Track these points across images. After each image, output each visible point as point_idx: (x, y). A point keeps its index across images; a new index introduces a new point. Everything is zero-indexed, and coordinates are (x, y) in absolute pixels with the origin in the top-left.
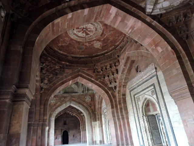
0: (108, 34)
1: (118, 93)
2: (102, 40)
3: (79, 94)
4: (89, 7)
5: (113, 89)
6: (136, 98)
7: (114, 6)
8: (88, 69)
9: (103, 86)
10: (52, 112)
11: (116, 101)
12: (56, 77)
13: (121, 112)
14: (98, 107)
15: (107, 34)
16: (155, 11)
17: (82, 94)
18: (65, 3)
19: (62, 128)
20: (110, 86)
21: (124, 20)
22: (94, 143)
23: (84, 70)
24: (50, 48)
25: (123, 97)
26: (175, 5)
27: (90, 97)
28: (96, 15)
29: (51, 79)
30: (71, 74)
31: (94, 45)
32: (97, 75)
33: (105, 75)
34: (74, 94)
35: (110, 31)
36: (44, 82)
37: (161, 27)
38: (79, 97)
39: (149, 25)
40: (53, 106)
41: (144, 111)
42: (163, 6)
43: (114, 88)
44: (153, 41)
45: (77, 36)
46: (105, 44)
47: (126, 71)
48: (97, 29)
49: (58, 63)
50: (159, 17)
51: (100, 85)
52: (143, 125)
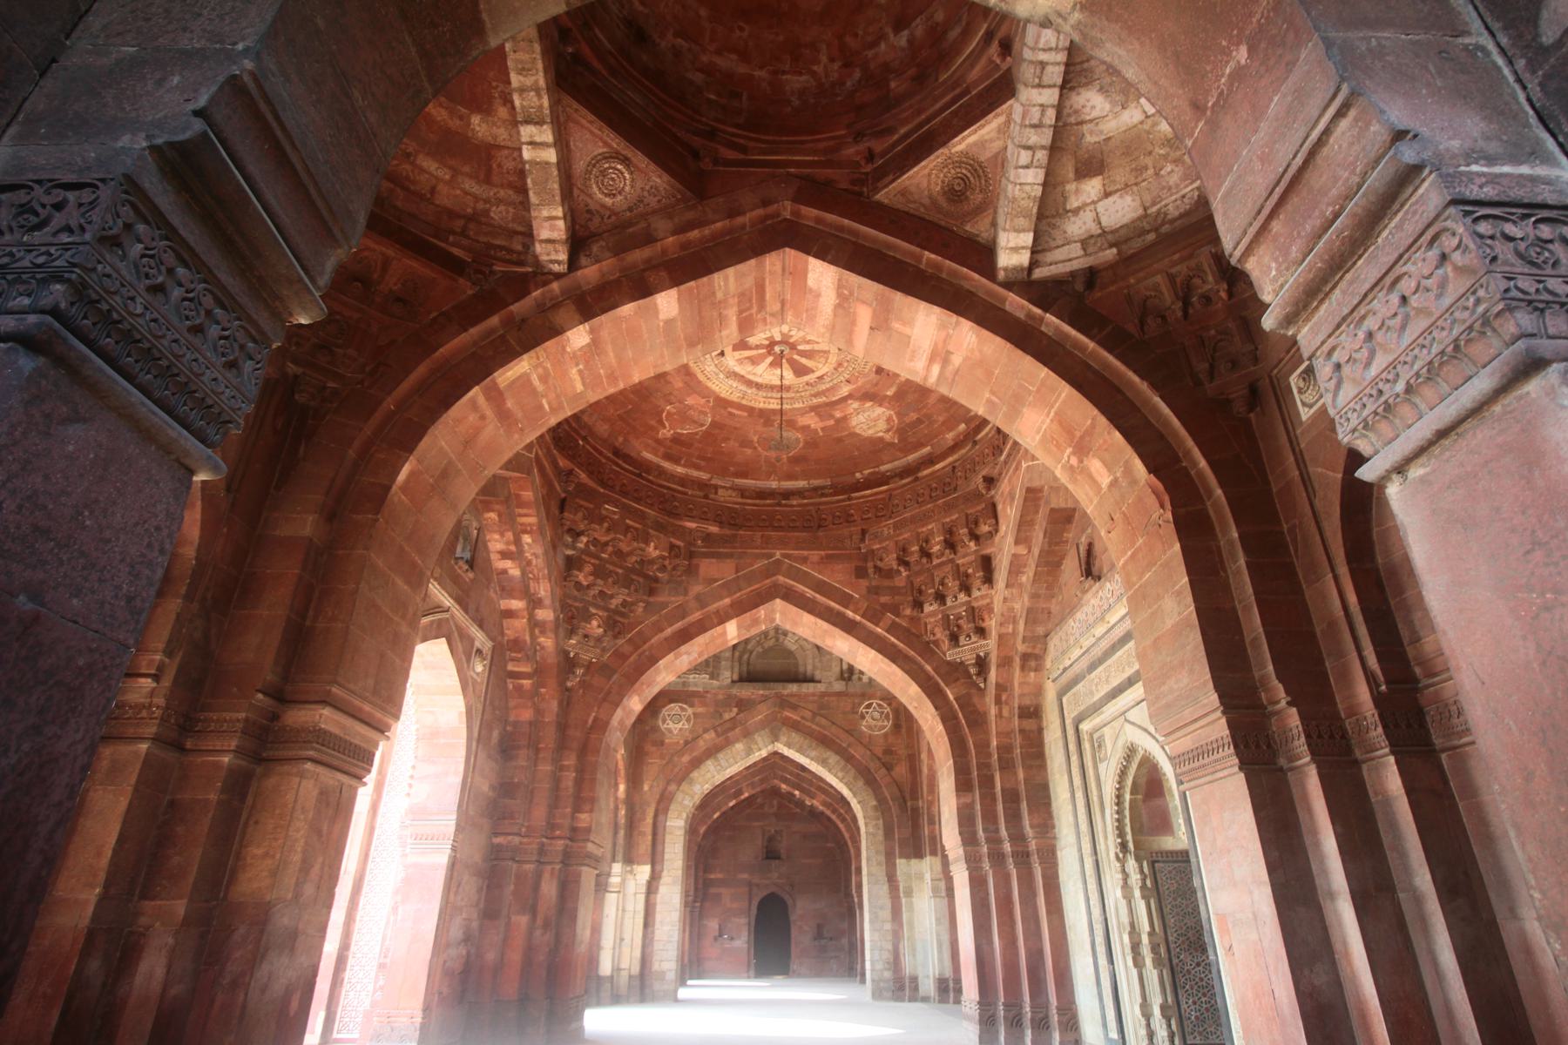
1: (998, 701)
3: (821, 688)
4: (676, 282)
5: (970, 676)
6: (1085, 737)
7: (820, 256)
8: (828, 557)
10: (672, 787)
11: (983, 747)
12: (648, 603)
13: (1014, 817)
16: (1058, 254)
17: (839, 686)
18: (545, 283)
19: (756, 880)
20: (951, 655)
21: (887, 320)
22: (901, 988)
23: (804, 560)
24: (617, 452)
25: (1029, 724)
26: (1173, 212)
28: (735, 309)
29: (623, 615)
30: (729, 588)
31: (854, 422)
32: (874, 591)
33: (920, 592)
34: (793, 688)
36: (581, 632)
37: (1091, 345)
38: (823, 705)
39: (1022, 336)
40: (680, 753)
42: (1105, 221)
43: (973, 671)
44: (1060, 423)
45: (749, 383)
46: (914, 416)
49: (660, 527)
50: (1079, 287)
51: (893, 645)
52: (1124, 911)
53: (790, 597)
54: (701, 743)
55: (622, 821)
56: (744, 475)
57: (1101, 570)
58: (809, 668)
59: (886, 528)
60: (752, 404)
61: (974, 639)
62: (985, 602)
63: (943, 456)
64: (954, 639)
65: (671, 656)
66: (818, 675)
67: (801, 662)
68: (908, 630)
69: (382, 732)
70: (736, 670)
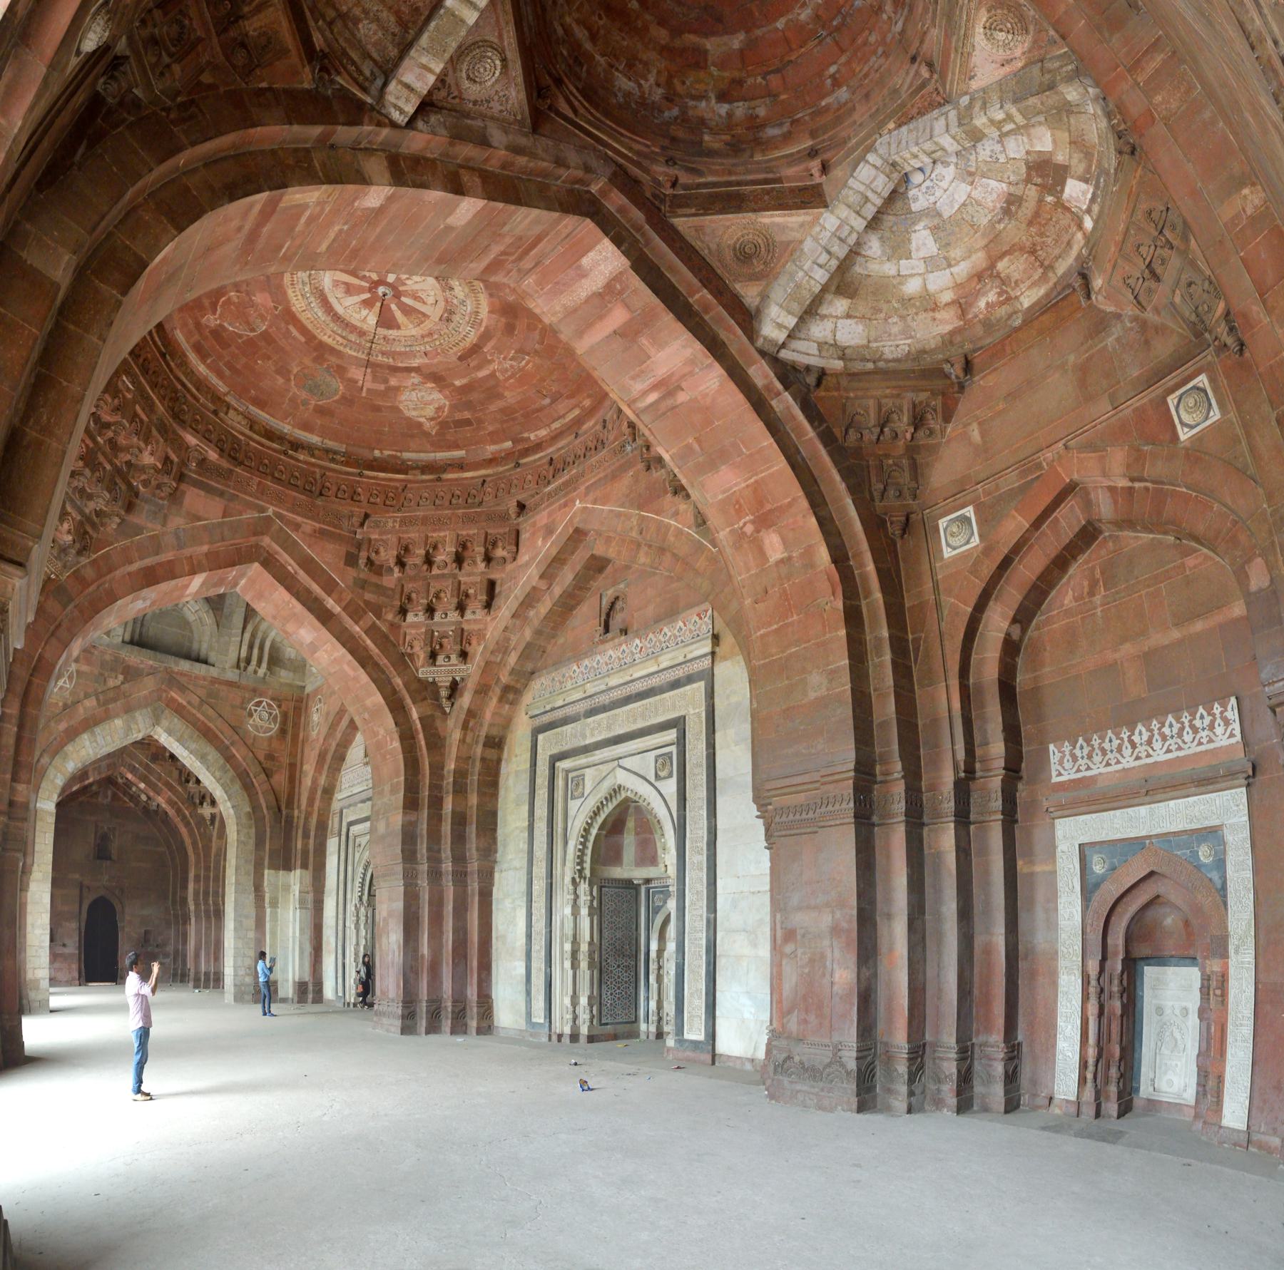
0: (507, 364)
1: (465, 727)
2: (458, 383)
3: (214, 672)
5: (436, 697)
8: (322, 532)
9: (384, 661)
11: (437, 769)
14: (315, 781)
15: (500, 364)
20: (425, 672)
25: (492, 754)
27: (276, 711)
32: (362, 585)
33: (409, 599)
34: (185, 665)
35: (521, 351)
41: (589, 852)
47: (544, 607)
48: (451, 313)
51: (366, 649)
53: (269, 563)
59: (391, 520)
62: (476, 627)
64: (433, 656)
68: (385, 636)
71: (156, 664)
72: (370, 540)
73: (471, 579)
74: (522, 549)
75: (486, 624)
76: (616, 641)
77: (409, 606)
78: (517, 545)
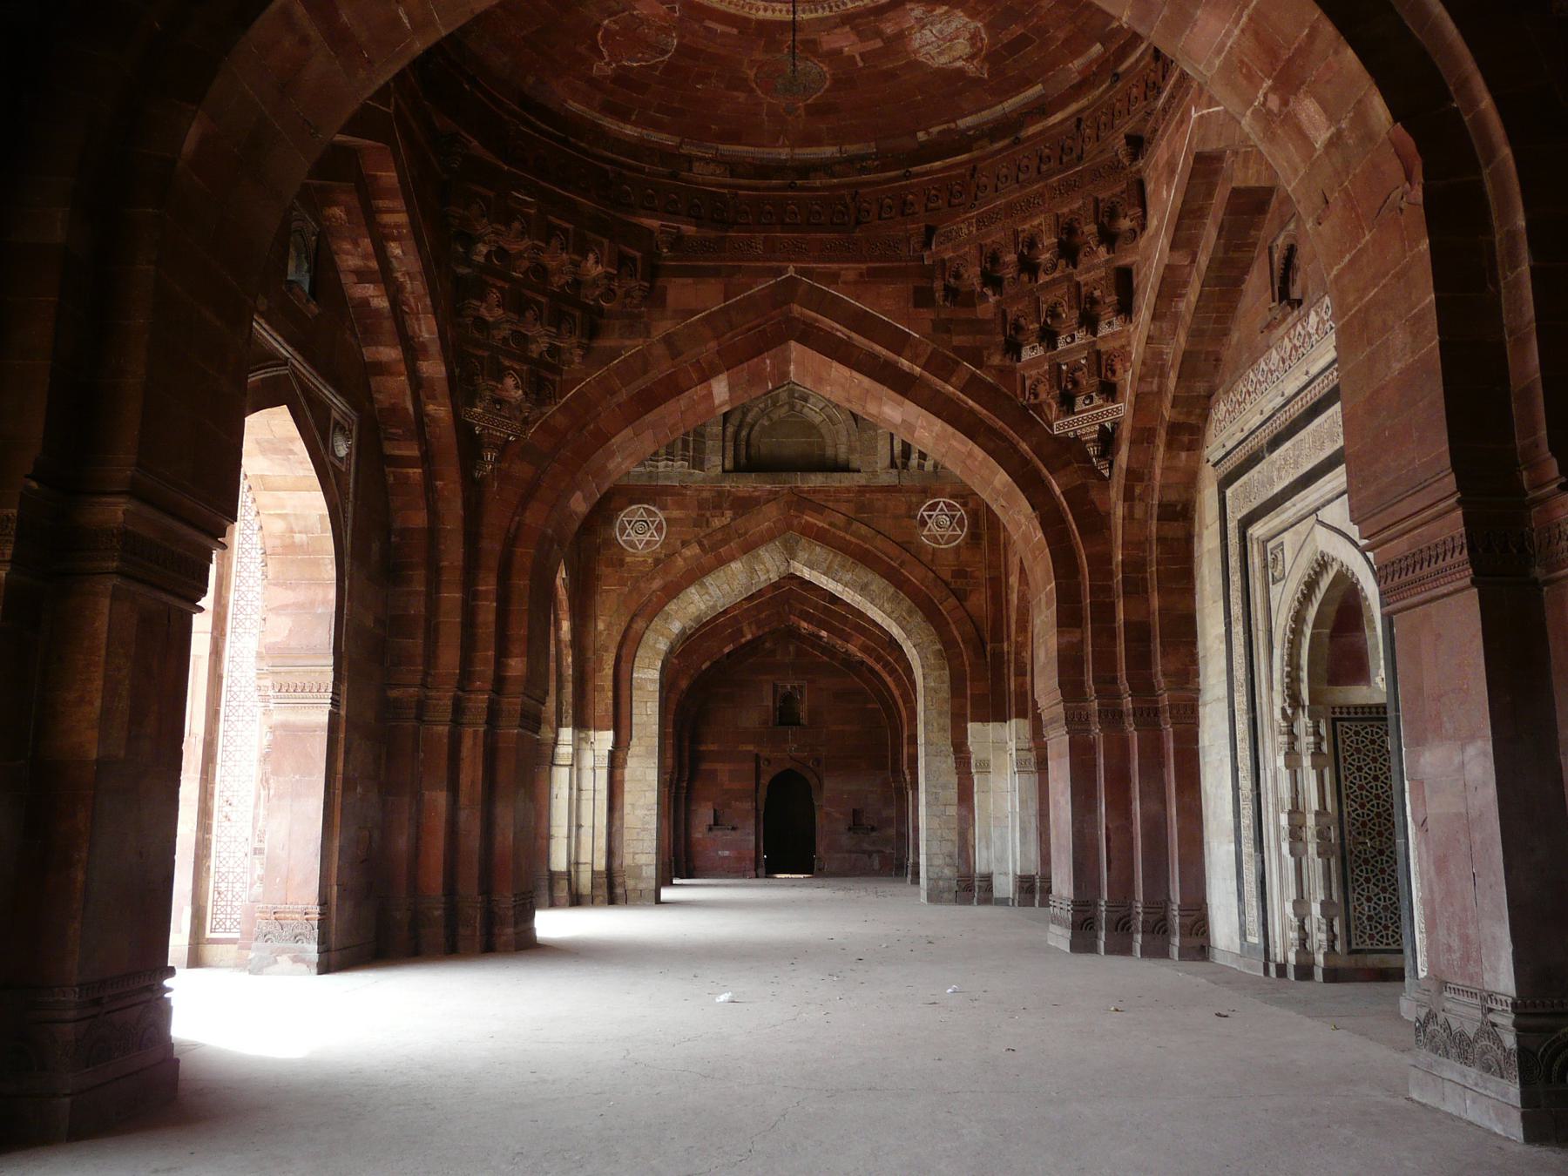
1: (1129, 496)
3: (859, 479)
8: (872, 273)
10: (639, 624)
11: (1101, 563)
12: (587, 350)
13: (1140, 661)
20: (1061, 427)
22: (969, 888)
23: (833, 278)
25: (1174, 530)
32: (943, 327)
33: (1018, 328)
34: (816, 480)
38: (864, 503)
43: (1092, 450)
46: (1016, 30)
51: (971, 410)
54: (680, 562)
55: (569, 672)
56: (735, 138)
57: (1304, 293)
58: (843, 449)
60: (745, 12)
61: (1097, 401)
62: (1117, 344)
63: (1061, 103)
65: (628, 432)
66: (855, 461)
67: (829, 441)
69: (215, 538)
70: (730, 454)
71: (777, 487)
72: (943, 260)
73: (1093, 275)
74: (1150, 211)
75: (1129, 337)
76: (1290, 319)
77: (1020, 338)
78: (1143, 205)
